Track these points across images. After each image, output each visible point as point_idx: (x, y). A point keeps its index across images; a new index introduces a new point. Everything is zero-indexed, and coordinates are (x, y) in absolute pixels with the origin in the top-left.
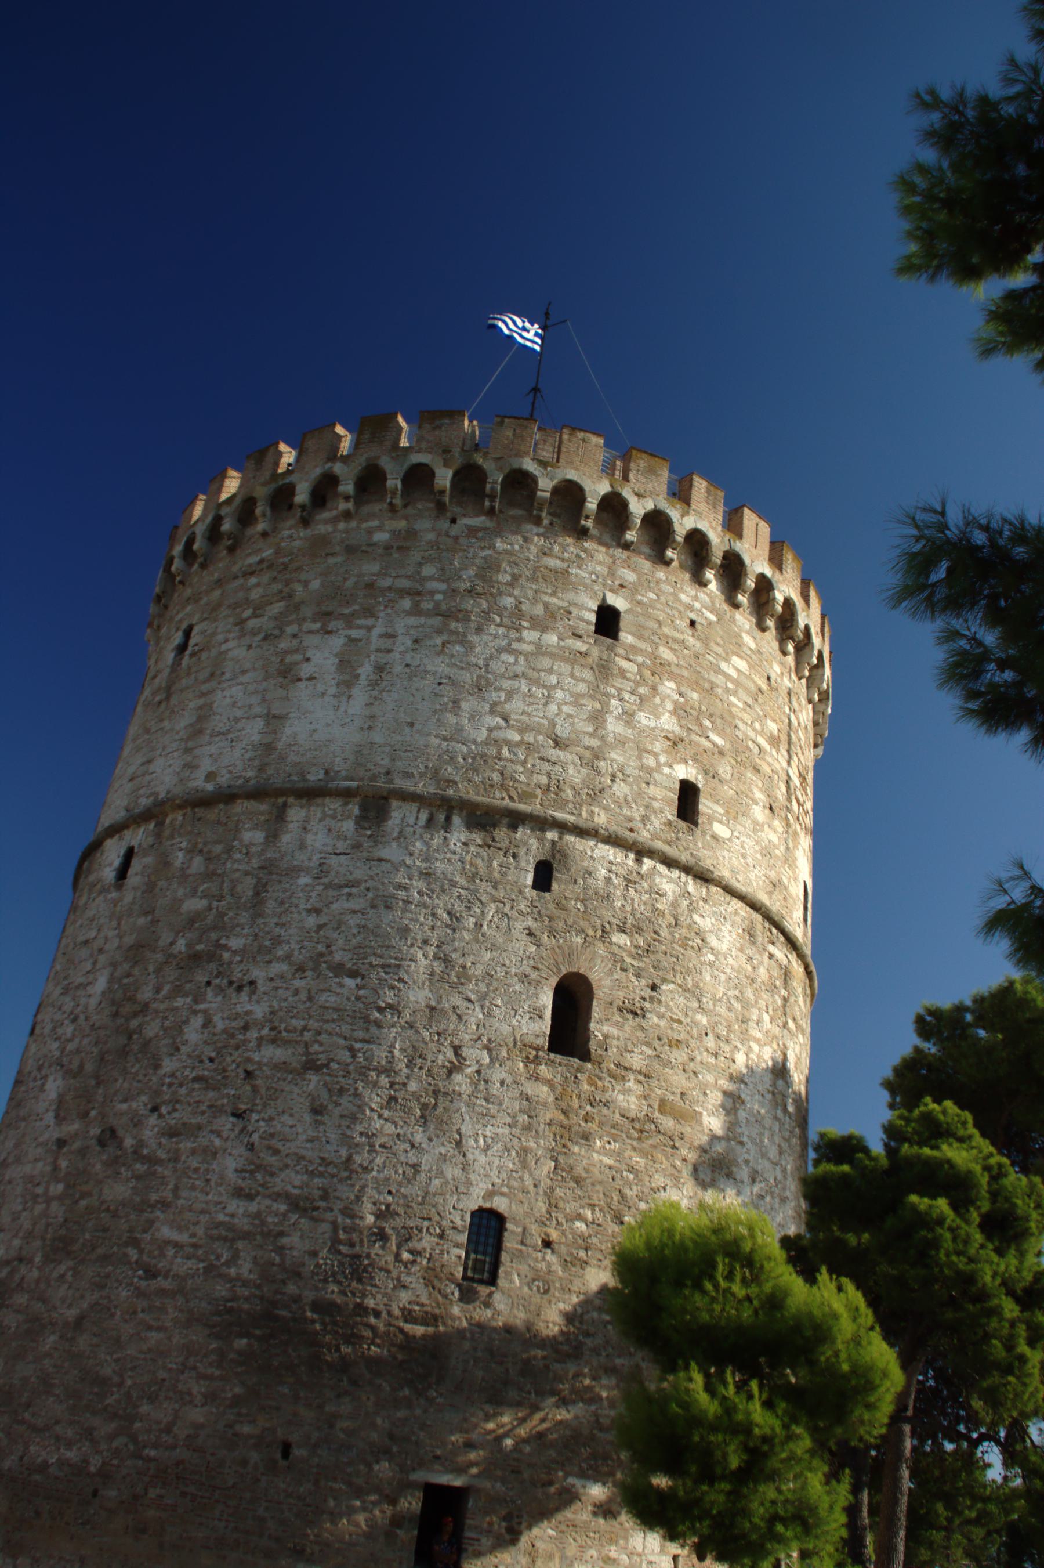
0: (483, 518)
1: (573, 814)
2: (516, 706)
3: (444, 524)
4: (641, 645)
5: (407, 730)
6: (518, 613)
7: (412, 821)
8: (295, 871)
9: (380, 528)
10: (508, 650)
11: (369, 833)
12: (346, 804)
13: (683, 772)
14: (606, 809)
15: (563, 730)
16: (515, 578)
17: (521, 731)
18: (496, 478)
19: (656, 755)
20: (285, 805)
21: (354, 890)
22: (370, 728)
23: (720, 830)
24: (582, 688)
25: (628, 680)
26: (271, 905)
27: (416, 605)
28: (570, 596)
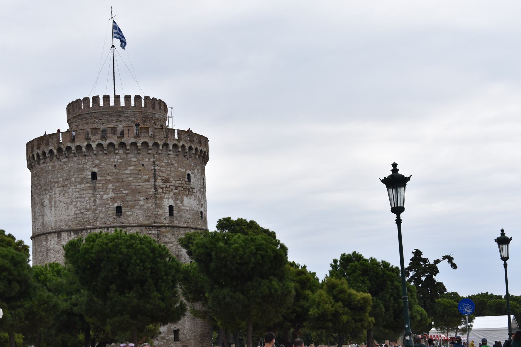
0: (66, 159)
1: (92, 225)
2: (78, 205)
3: (59, 162)
4: (102, 178)
5: (61, 215)
6: (76, 182)
7: (65, 235)
8: (51, 249)
9: (49, 166)
10: (75, 192)
11: (59, 240)
12: (55, 234)
13: (116, 205)
14: (99, 221)
15: (88, 207)
16: (74, 172)
17: (80, 210)
18: (64, 149)
19: (109, 204)
20: (47, 236)
21: (59, 252)
22: (56, 217)
23: (128, 213)
24: (90, 195)
25: (101, 189)
26: (49, 257)
27: (58, 185)
28: (85, 173)
